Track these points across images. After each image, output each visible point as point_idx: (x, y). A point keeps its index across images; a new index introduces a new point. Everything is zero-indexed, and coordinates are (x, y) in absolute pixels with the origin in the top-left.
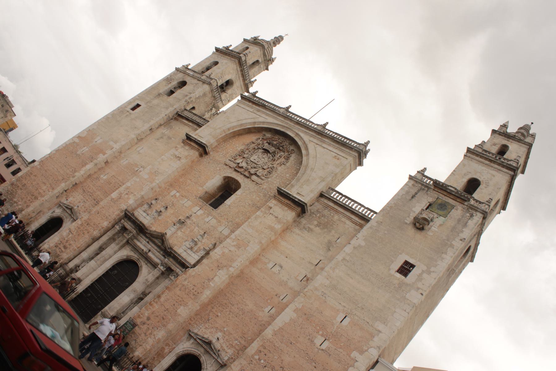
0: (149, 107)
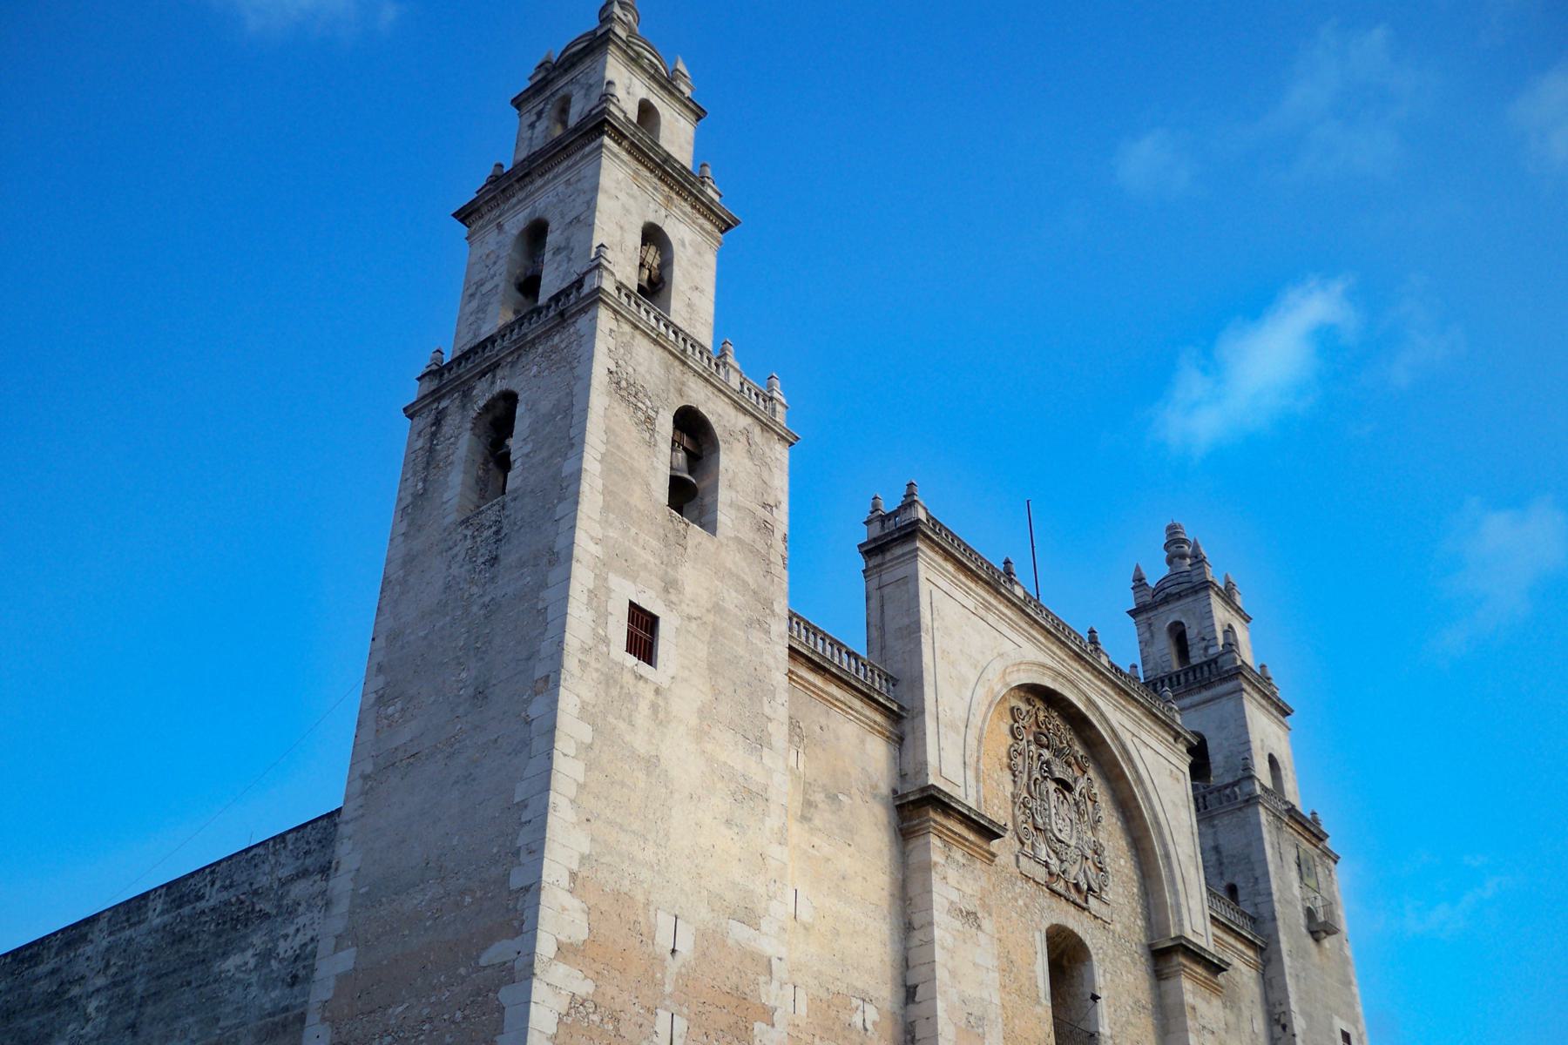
0: (693, 626)
